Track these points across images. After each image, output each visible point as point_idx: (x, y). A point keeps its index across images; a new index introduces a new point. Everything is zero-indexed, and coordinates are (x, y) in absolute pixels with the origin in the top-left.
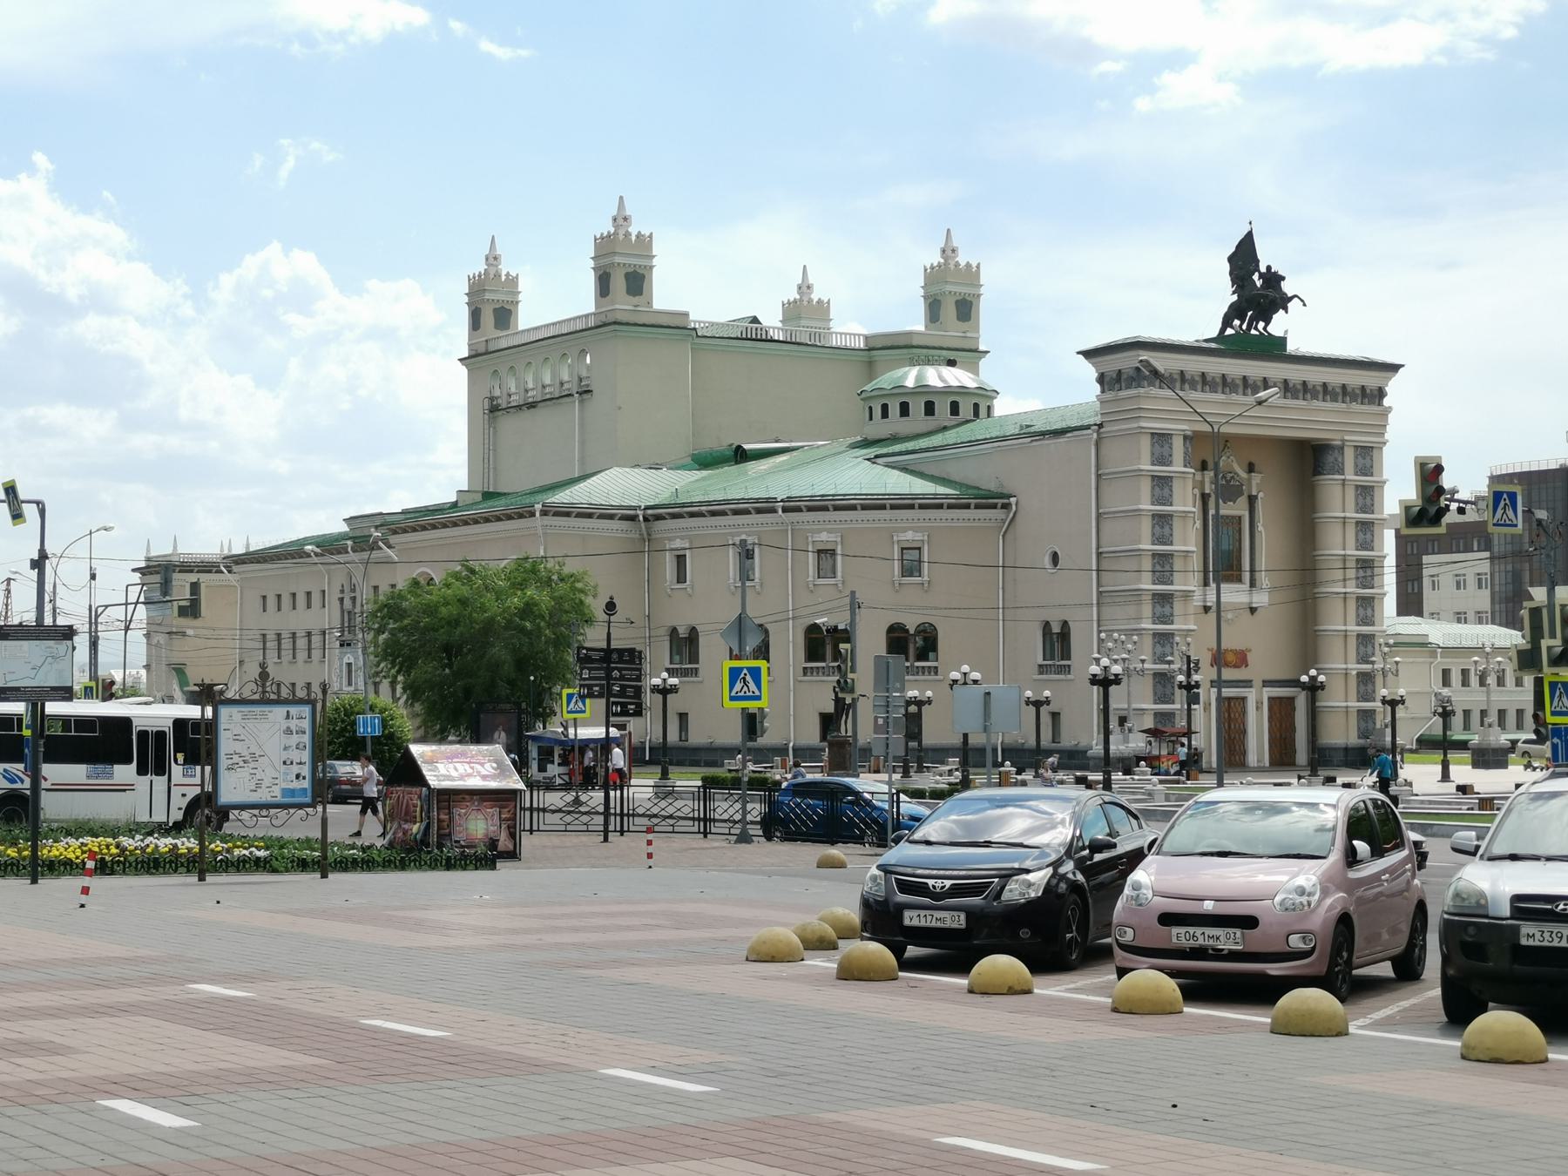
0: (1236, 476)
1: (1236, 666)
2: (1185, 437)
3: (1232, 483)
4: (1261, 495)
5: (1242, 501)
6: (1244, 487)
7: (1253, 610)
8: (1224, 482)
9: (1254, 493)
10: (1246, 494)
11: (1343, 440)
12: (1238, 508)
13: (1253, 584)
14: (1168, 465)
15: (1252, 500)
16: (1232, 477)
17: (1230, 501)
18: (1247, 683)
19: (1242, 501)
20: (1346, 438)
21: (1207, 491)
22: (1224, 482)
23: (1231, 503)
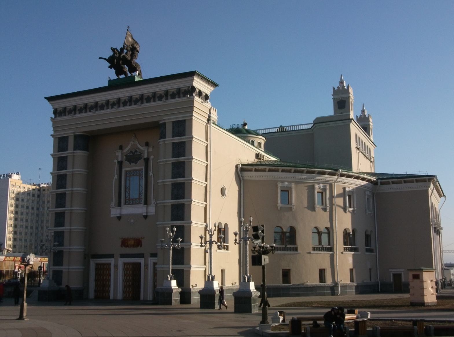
0: (138, 150)
1: (134, 246)
2: (76, 137)
3: (136, 154)
4: (152, 157)
5: (141, 162)
6: (142, 155)
7: (146, 217)
8: (131, 154)
9: (146, 156)
10: (143, 159)
11: (164, 120)
12: (140, 166)
13: (146, 203)
14: (66, 151)
15: (147, 160)
16: (136, 151)
17: (133, 162)
18: (141, 255)
19: (141, 162)
20: (164, 118)
21: (120, 160)
22: (131, 154)
23: (134, 164)
